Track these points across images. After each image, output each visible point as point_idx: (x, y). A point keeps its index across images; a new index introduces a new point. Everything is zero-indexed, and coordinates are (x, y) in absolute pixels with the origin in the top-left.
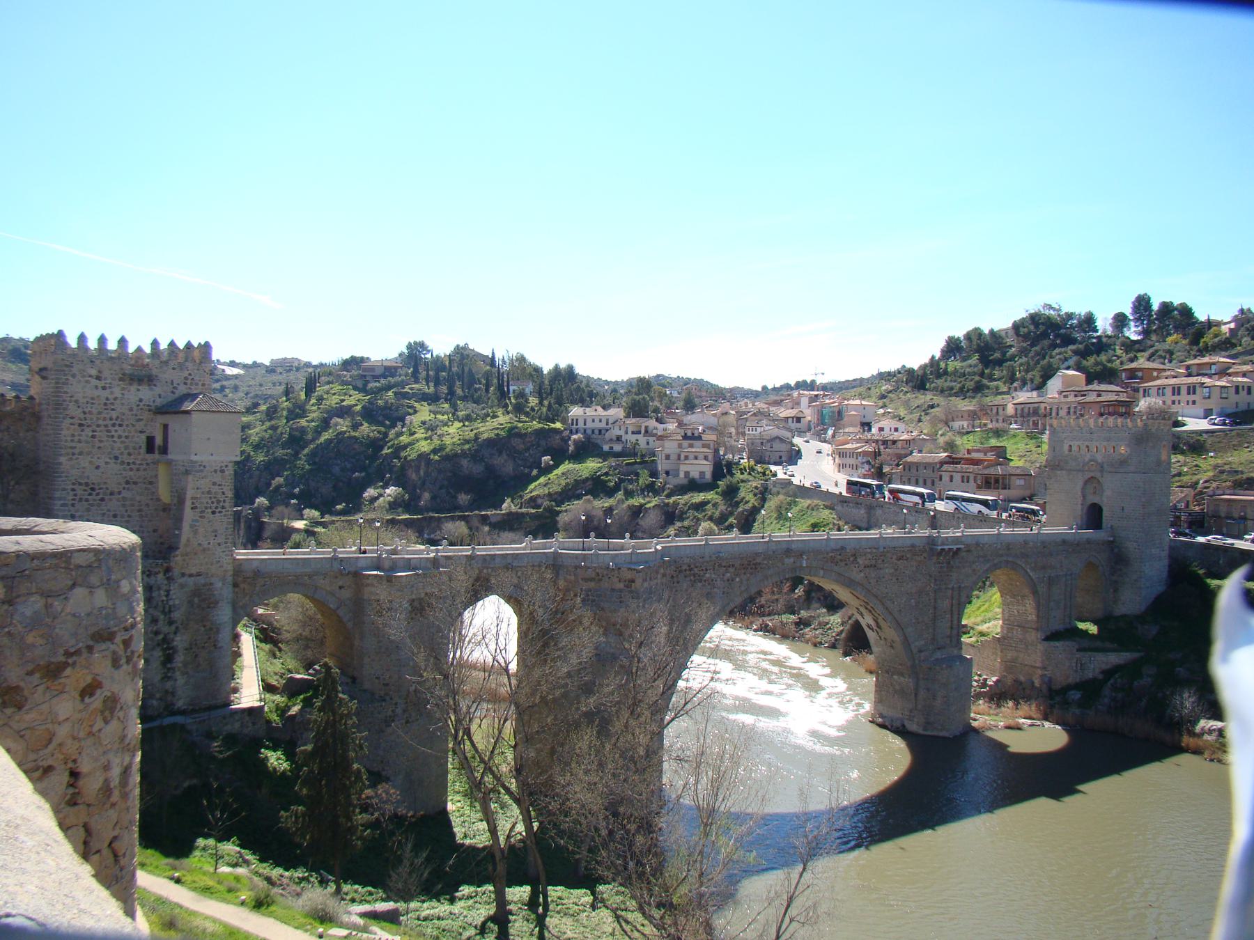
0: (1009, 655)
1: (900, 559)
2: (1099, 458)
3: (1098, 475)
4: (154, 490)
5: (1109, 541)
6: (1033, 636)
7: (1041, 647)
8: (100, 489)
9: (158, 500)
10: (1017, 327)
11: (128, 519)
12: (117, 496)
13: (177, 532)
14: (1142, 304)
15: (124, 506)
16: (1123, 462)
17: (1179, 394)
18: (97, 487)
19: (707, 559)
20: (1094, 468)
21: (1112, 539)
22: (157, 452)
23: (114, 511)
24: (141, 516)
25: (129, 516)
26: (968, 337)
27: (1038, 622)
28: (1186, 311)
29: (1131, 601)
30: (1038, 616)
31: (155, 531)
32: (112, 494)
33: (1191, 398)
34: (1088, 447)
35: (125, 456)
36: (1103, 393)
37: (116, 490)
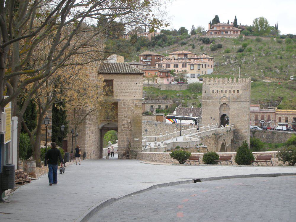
2: (227, 95)
3: (227, 103)
13: (136, 139)
16: (239, 97)
17: (177, 67)
21: (235, 129)
33: (184, 69)
34: (222, 91)
36: (139, 66)
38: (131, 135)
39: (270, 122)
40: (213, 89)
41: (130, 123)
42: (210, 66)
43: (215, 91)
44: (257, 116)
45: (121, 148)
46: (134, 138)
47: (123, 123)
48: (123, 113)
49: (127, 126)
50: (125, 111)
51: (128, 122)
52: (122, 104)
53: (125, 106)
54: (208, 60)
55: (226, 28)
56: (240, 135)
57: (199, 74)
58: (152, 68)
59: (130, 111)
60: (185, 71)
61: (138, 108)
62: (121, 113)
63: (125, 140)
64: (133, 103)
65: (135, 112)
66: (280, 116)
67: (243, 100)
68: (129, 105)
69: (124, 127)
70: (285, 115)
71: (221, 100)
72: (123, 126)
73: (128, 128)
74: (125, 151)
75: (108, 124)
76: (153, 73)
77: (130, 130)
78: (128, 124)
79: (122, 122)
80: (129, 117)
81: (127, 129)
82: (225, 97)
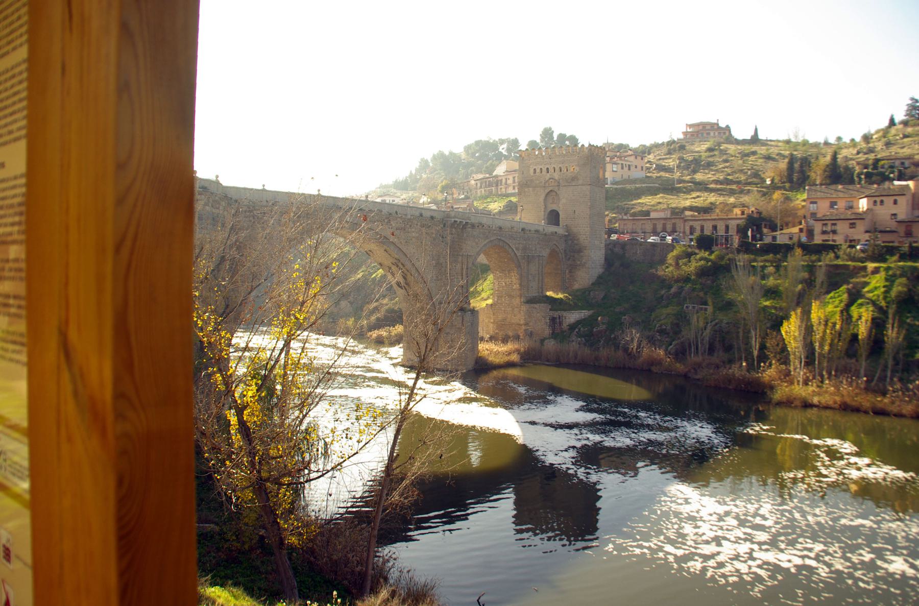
0: (500, 317)
1: (423, 226)
2: (556, 176)
3: (556, 189)
5: (565, 235)
6: (517, 301)
7: (524, 308)
10: (467, 149)
14: (547, 133)
16: (574, 179)
19: (265, 203)
20: (553, 184)
21: (567, 234)
26: (435, 158)
27: (520, 290)
28: (574, 140)
29: (584, 278)
30: (520, 285)
34: (548, 169)
39: (676, 234)
40: (534, 167)
43: (538, 171)
44: (655, 225)
55: (708, 127)
56: (577, 245)
66: (691, 223)
67: (580, 182)
70: (699, 222)
71: (547, 184)
82: (552, 179)
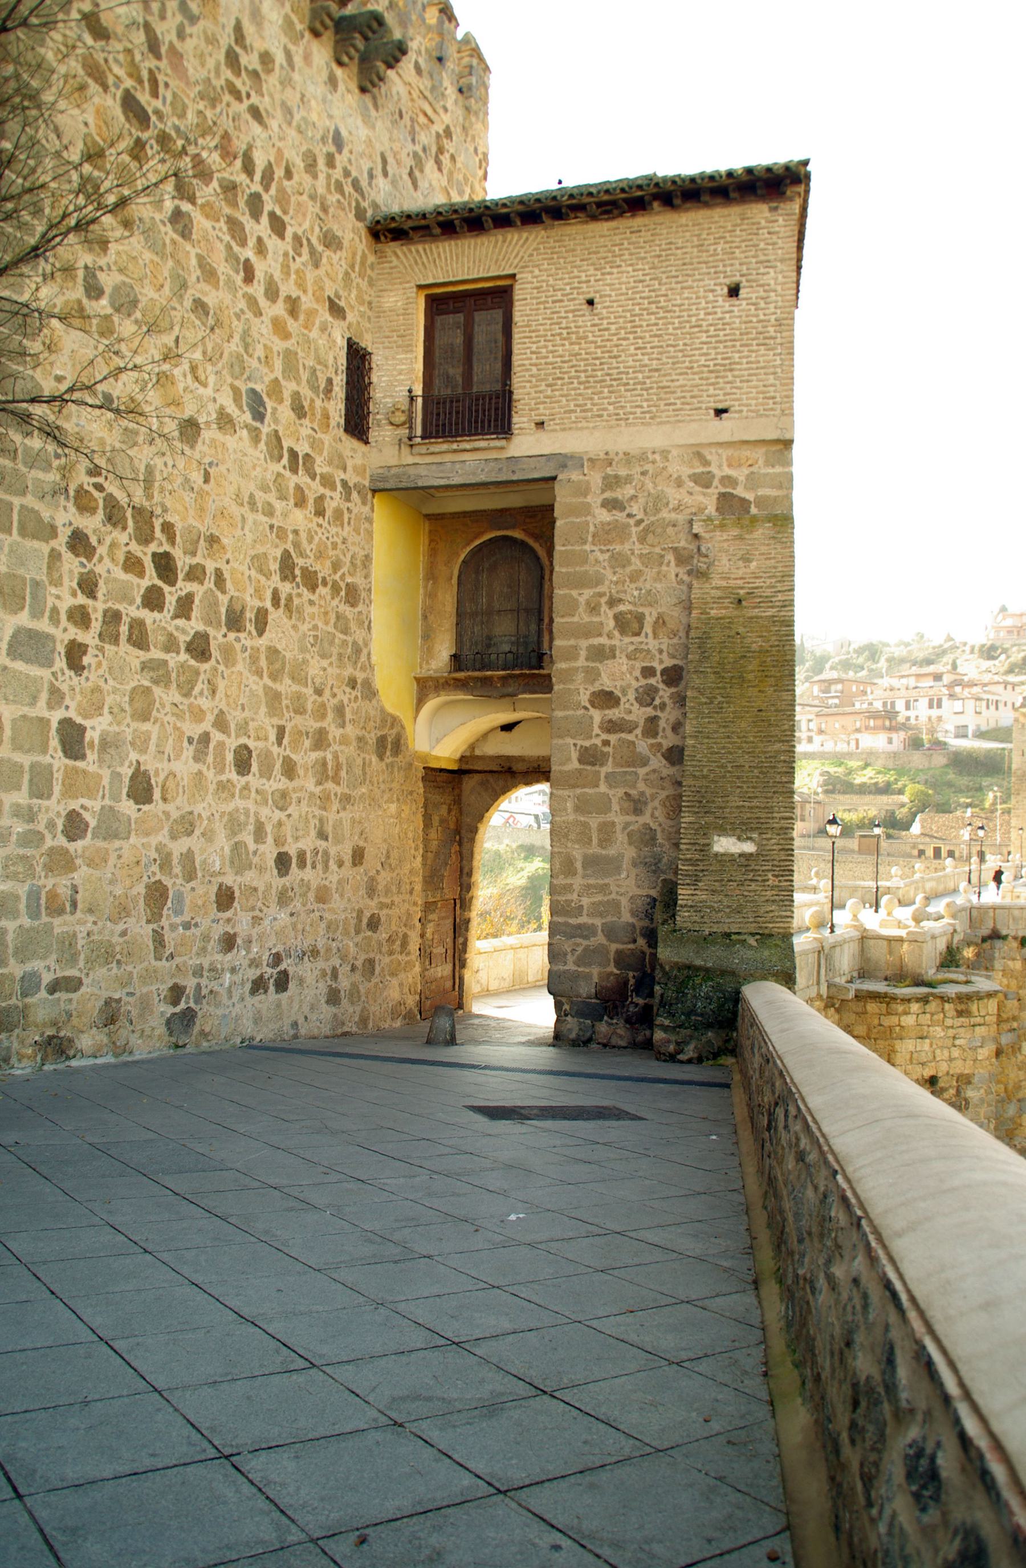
4: (359, 635)
8: (195, 574)
9: (370, 692)
11: (283, 783)
12: (248, 639)
13: (725, 845)
15: (274, 698)
18: (182, 562)
22: (382, 433)
23: (243, 728)
24: (323, 773)
25: (289, 770)
31: (358, 856)
32: (234, 621)
33: (935, 713)
35: (285, 412)
37: (253, 603)
38: (675, 807)
41: (673, 676)
42: (1009, 705)
45: (584, 931)
46: (705, 831)
47: (606, 683)
48: (599, 581)
49: (639, 714)
50: (619, 561)
51: (648, 672)
52: (594, 500)
53: (620, 516)
54: (1002, 686)
57: (978, 726)
58: (848, 709)
59: (670, 557)
60: (940, 719)
61: (754, 520)
62: (582, 582)
63: (623, 849)
64: (704, 481)
65: (724, 564)
68: (658, 502)
69: (612, 726)
72: (597, 716)
73: (651, 726)
74: (620, 959)
75: (508, 728)
76: (848, 721)
77: (675, 755)
78: (647, 696)
79: (592, 675)
80: (660, 622)
81: (643, 746)
